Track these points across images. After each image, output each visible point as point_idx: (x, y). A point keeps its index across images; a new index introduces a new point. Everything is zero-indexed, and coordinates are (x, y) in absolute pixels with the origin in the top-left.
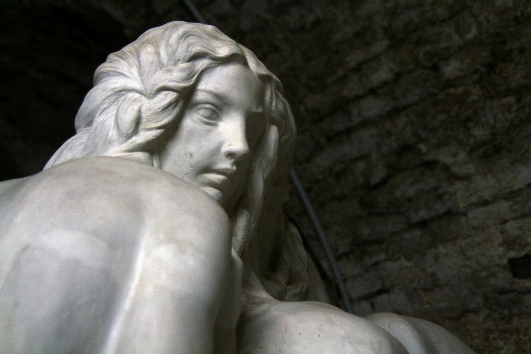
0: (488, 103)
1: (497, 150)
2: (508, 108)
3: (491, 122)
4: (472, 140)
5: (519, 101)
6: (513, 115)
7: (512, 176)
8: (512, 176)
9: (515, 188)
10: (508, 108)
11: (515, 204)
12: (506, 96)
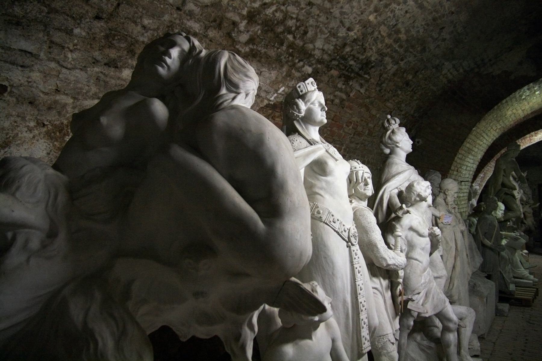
0: (36, 3)
1: (18, 24)
2: (41, 12)
3: (28, 11)
4: (11, 11)
5: (48, 13)
6: (40, 16)
7: (15, 40)
8: (15, 40)
9: (12, 47)
10: (41, 12)
11: (5, 53)
12: (46, 7)
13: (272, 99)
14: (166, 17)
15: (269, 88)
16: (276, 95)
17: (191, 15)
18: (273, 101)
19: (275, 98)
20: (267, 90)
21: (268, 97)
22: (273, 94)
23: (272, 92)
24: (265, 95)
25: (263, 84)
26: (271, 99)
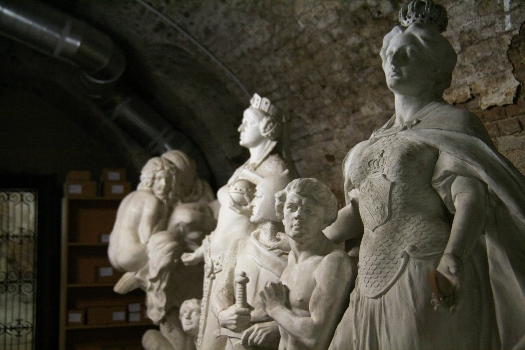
13: (509, 26)
14: (337, 54)
15: (482, 19)
16: (508, 17)
17: (341, 36)
18: (515, 29)
19: (512, 21)
20: (484, 24)
21: (497, 31)
22: (500, 21)
23: (497, 20)
24: (493, 33)
25: (471, 22)
26: (506, 29)
